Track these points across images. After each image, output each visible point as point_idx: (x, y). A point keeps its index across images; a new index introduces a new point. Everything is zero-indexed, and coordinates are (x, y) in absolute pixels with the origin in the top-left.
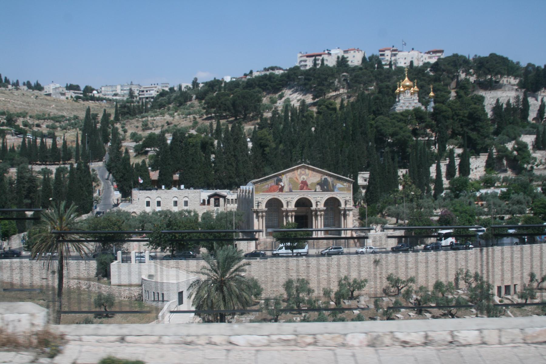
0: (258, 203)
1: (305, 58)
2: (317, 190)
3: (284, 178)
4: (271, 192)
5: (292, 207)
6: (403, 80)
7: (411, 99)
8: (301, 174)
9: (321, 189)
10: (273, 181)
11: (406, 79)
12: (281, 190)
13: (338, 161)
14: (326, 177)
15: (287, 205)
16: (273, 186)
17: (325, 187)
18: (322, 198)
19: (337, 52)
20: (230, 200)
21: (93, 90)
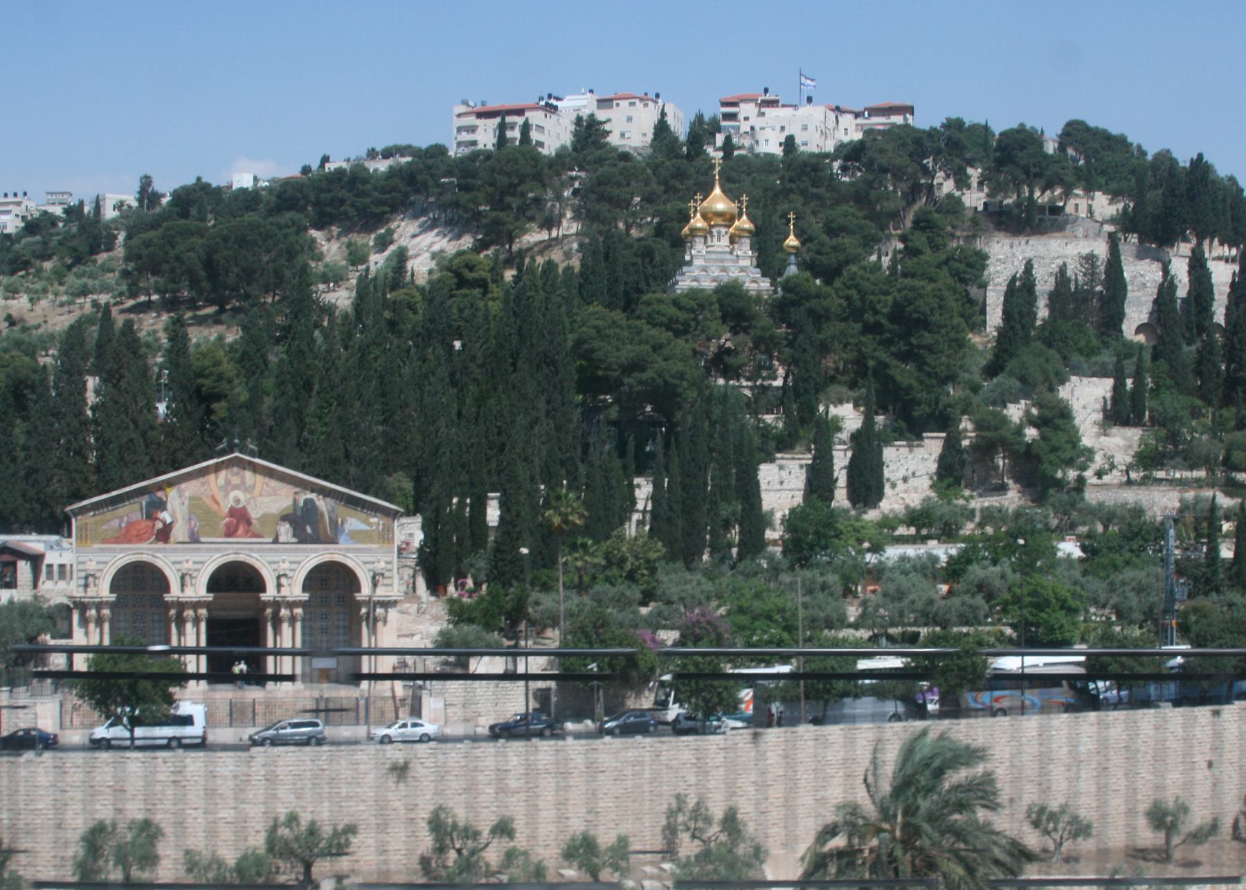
0: (86, 578)
1: (471, 120)
2: (282, 539)
3: (172, 496)
4: (129, 541)
5: (198, 590)
7: (728, 256)
9: (294, 535)
10: (136, 506)
11: (717, 191)
12: (164, 535)
13: (437, 449)
14: (313, 496)
15: (183, 585)
16: (137, 522)
17: (309, 530)
18: (299, 563)
19: (577, 104)
20: (56, 568)
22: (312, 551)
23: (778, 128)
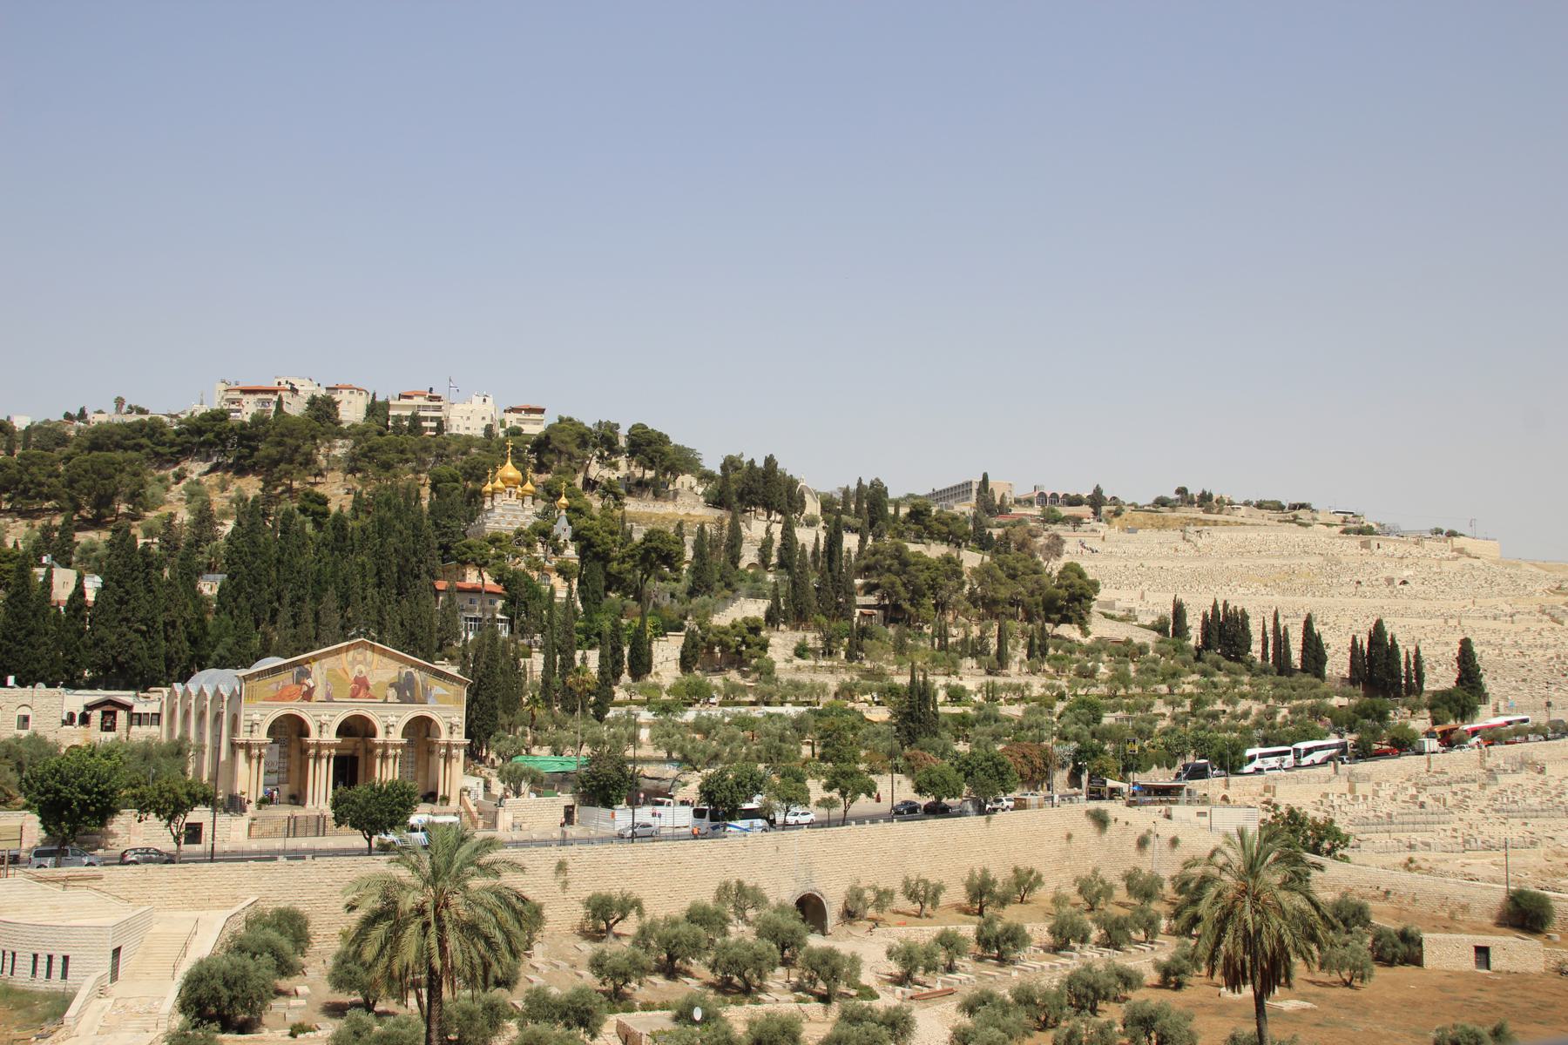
1: (237, 395)
4: (283, 700)
5: (330, 737)
6: (504, 464)
8: (354, 662)
11: (509, 463)
12: (308, 696)
14: (412, 670)
16: (289, 686)
17: (408, 694)
19: (307, 389)
22: (410, 708)
23: (465, 418)
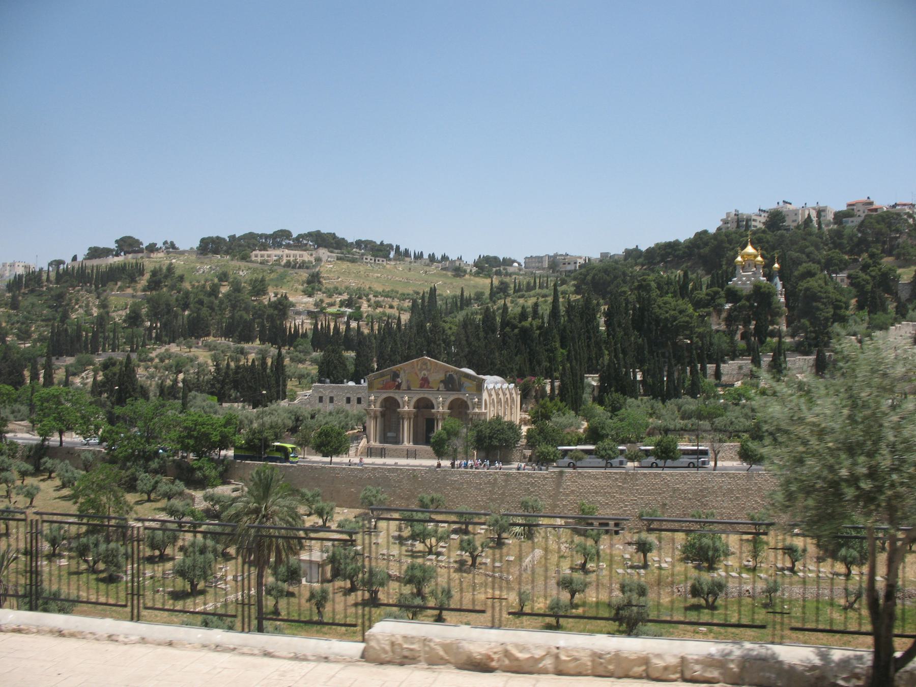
8: (421, 370)
12: (398, 387)
21: (514, 261)
